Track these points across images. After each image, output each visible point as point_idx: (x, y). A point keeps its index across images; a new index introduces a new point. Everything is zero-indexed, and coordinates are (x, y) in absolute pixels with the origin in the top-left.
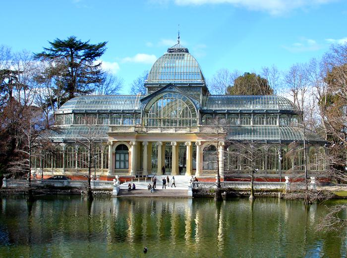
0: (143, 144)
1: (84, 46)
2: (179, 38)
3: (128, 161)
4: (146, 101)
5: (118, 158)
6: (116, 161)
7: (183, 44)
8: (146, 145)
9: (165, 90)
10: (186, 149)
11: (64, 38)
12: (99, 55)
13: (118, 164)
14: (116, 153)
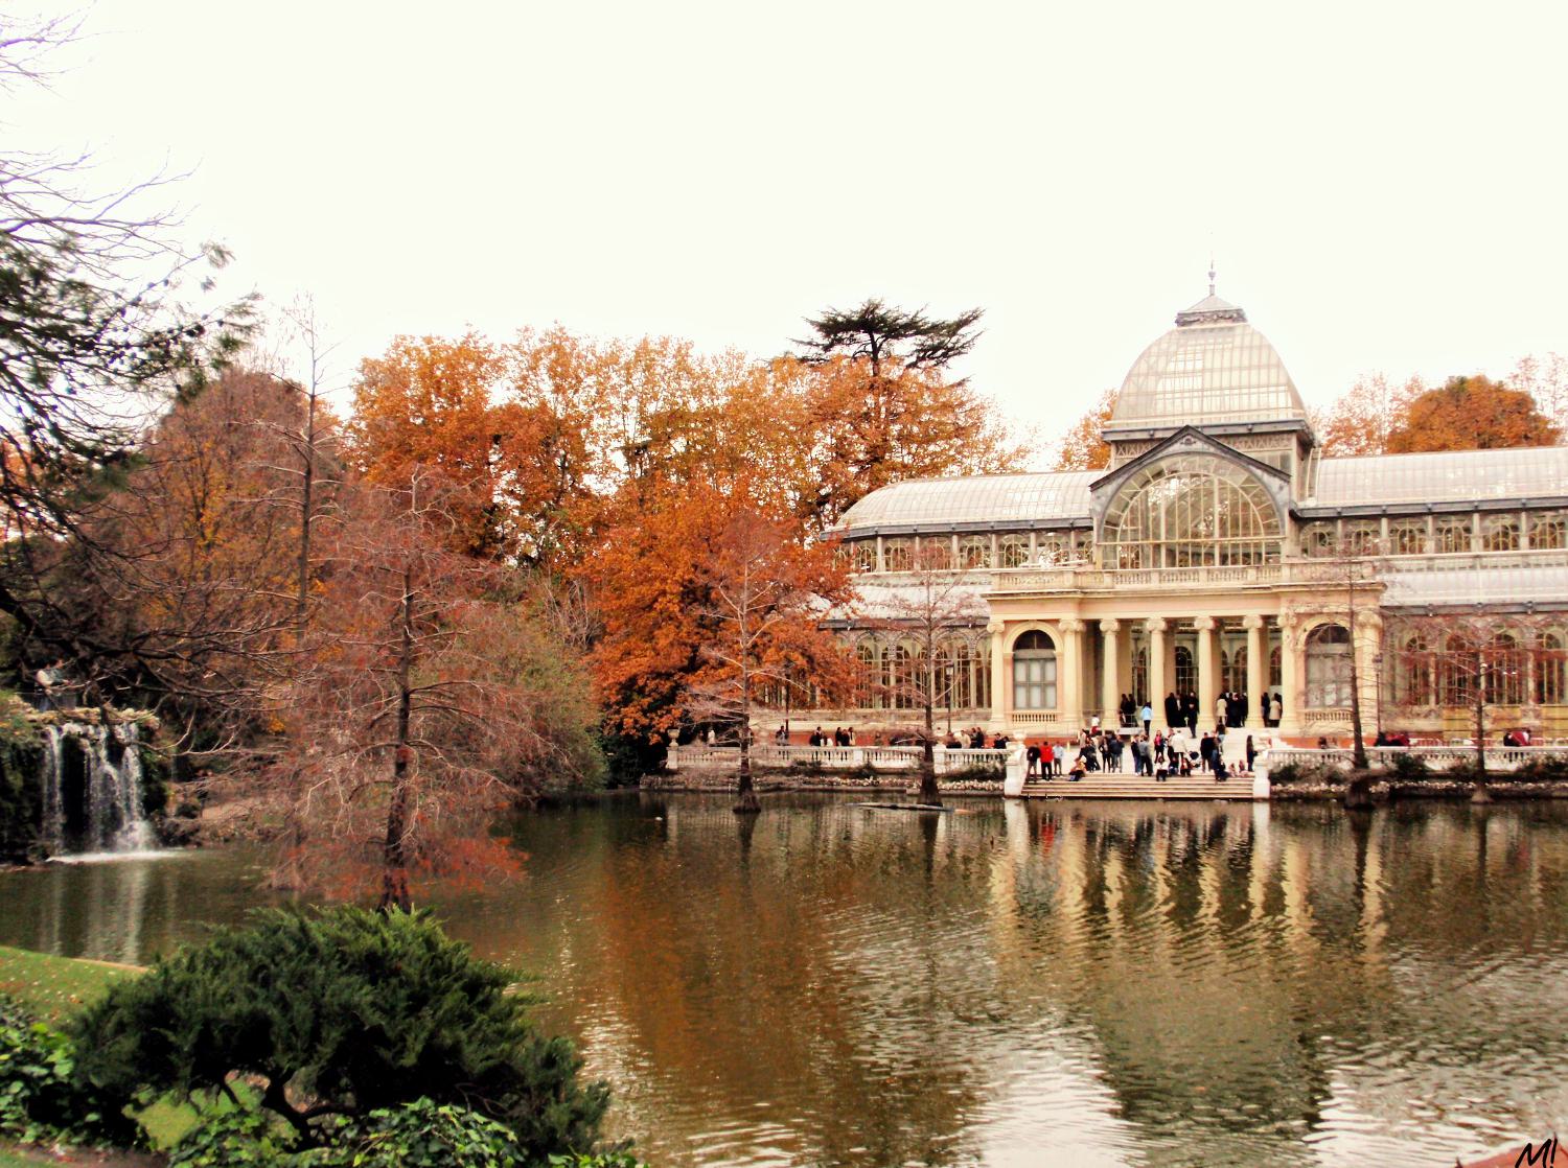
0: (1102, 627)
1: (913, 327)
2: (1212, 275)
3: (1054, 684)
4: (1109, 489)
5: (1021, 677)
6: (1015, 685)
7: (1229, 299)
8: (1109, 626)
9: (1171, 450)
10: (1246, 639)
11: (850, 306)
12: (957, 351)
13: (1021, 693)
14: (1015, 660)
